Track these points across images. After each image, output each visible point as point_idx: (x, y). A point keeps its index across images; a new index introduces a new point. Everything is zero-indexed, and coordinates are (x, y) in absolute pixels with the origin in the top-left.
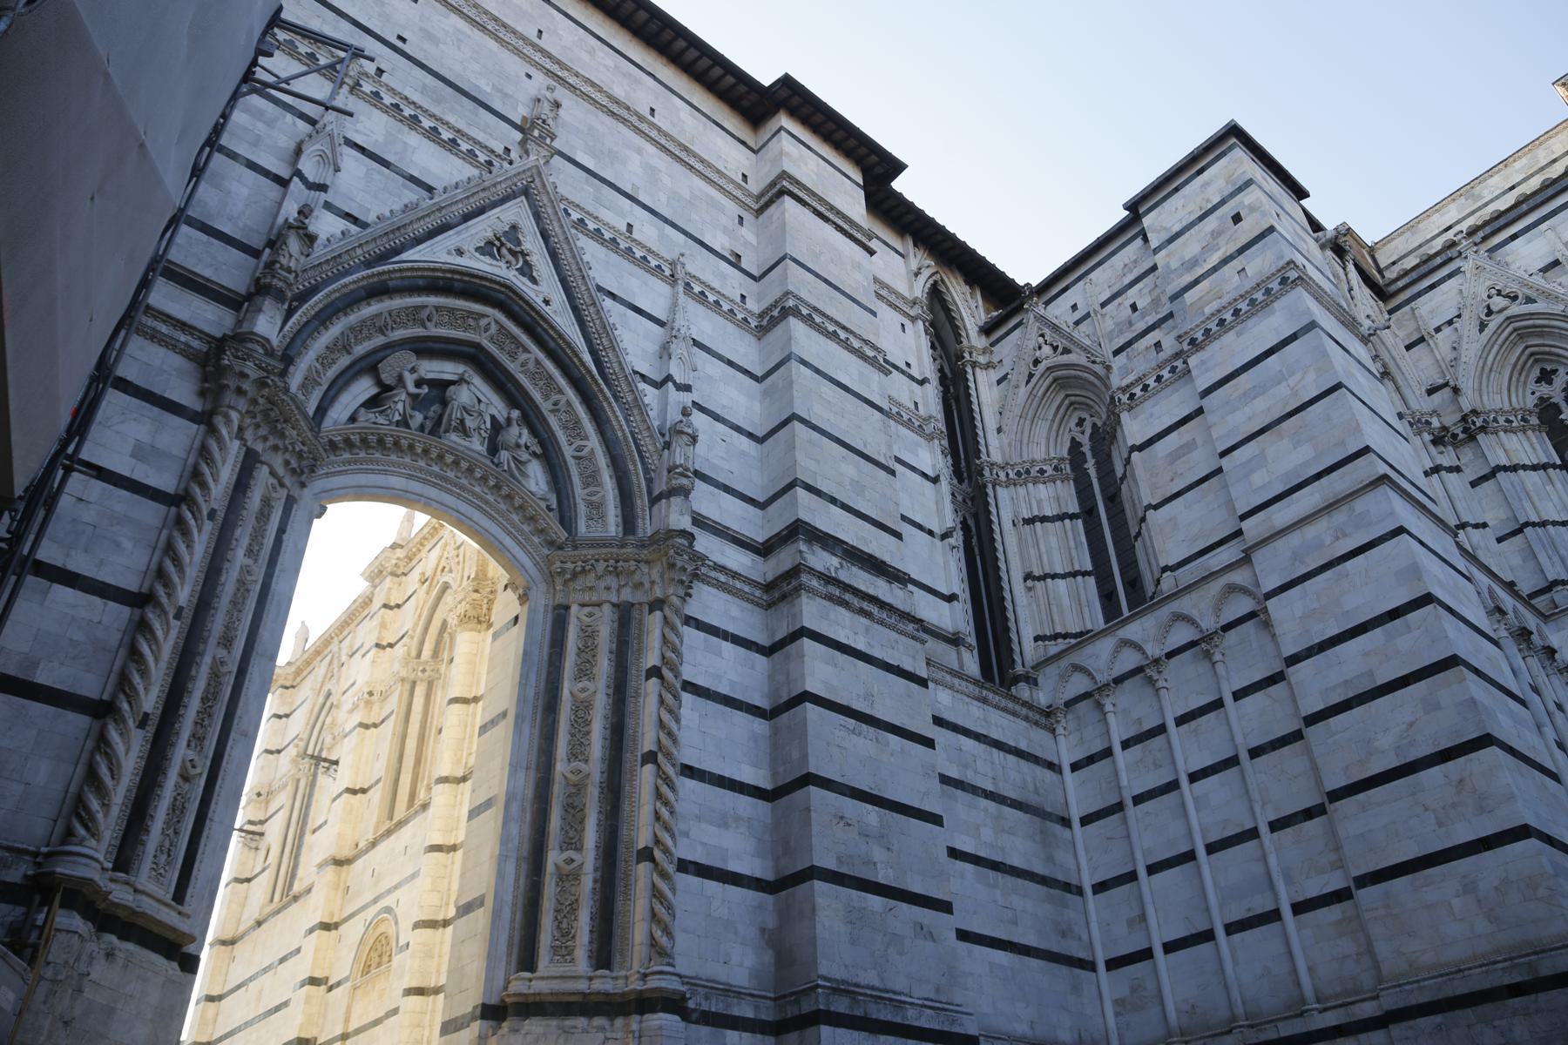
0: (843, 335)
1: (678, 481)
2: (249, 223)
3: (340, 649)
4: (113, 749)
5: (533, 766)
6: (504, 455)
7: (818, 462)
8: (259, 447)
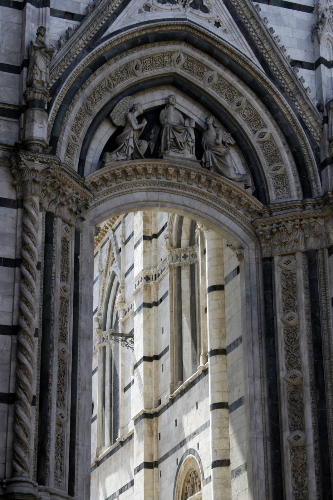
2: (7, 48)
3: (115, 237)
4: (23, 422)
5: (265, 375)
6: (208, 153)
8: (52, 209)
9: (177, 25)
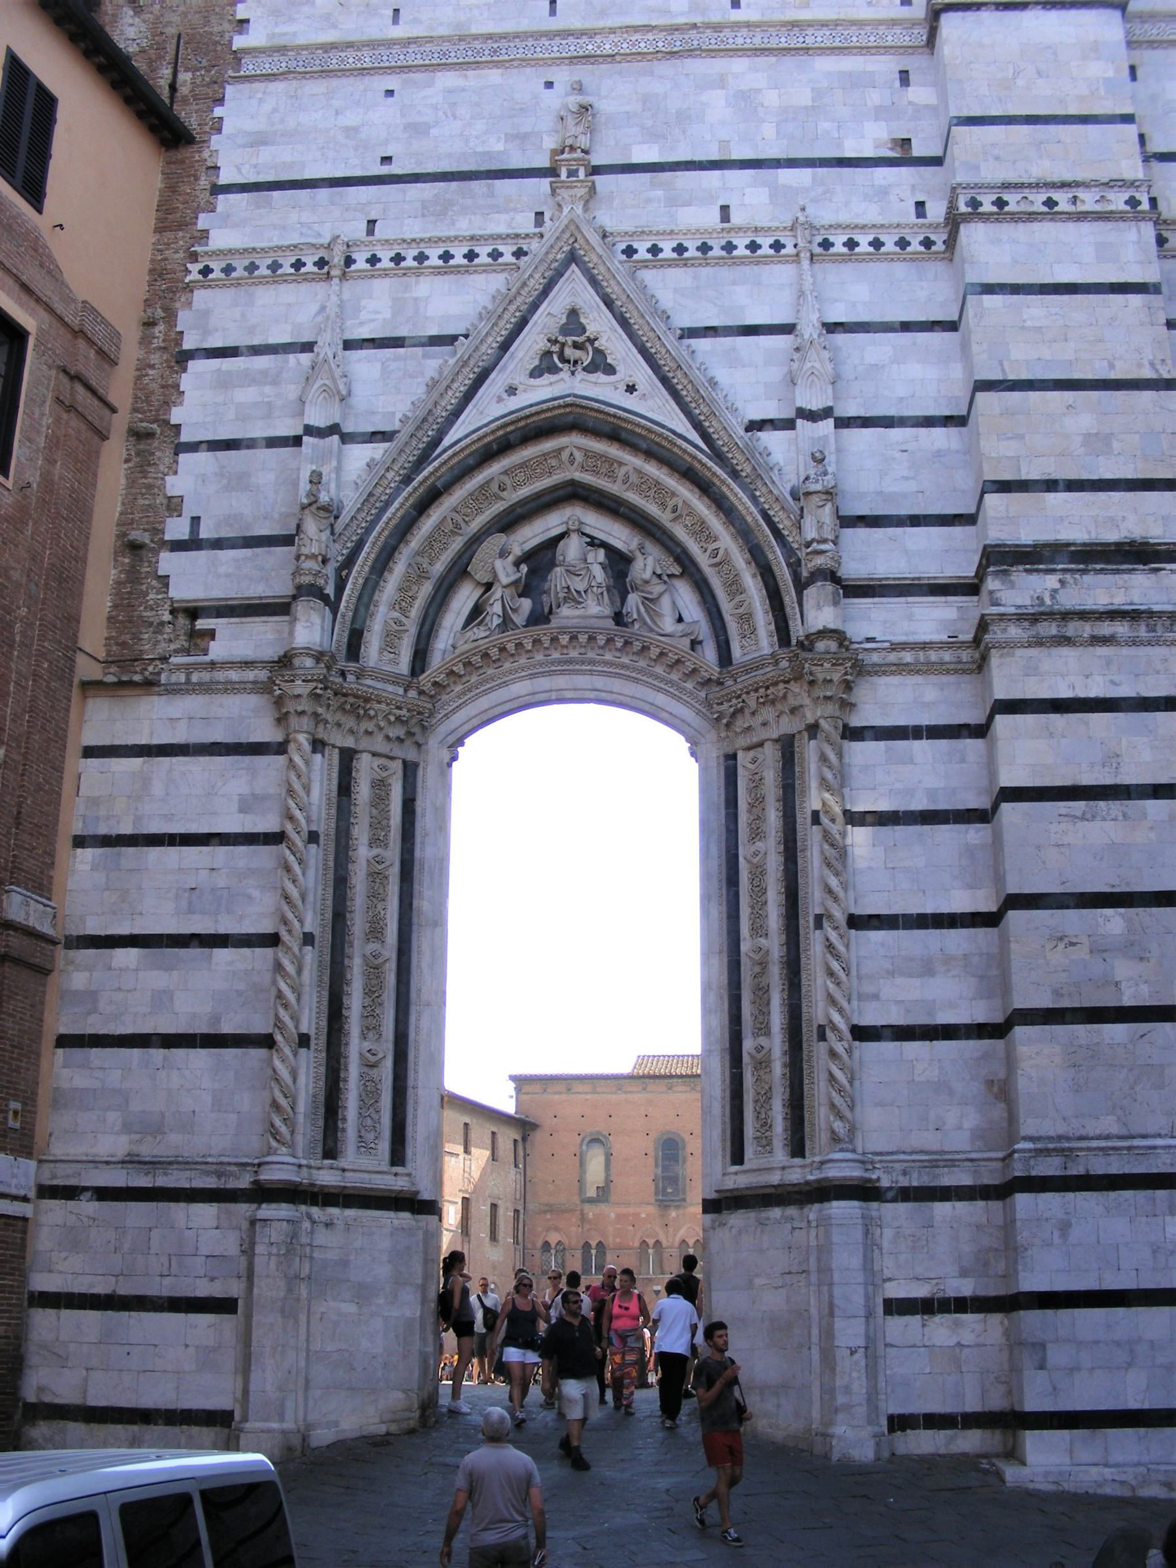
0: (1059, 196)
1: (813, 563)
2: (283, 510)
5: (725, 949)
6: (633, 599)
7: (1020, 437)
9: (554, 408)
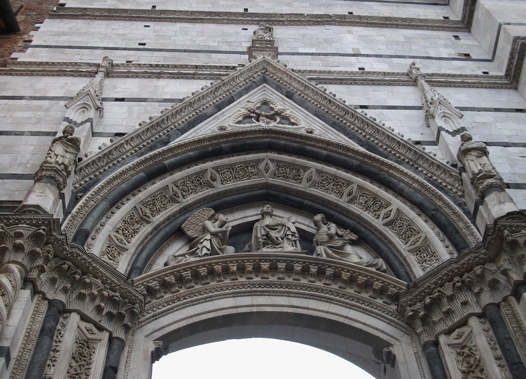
1: (485, 183)
6: (320, 249)
